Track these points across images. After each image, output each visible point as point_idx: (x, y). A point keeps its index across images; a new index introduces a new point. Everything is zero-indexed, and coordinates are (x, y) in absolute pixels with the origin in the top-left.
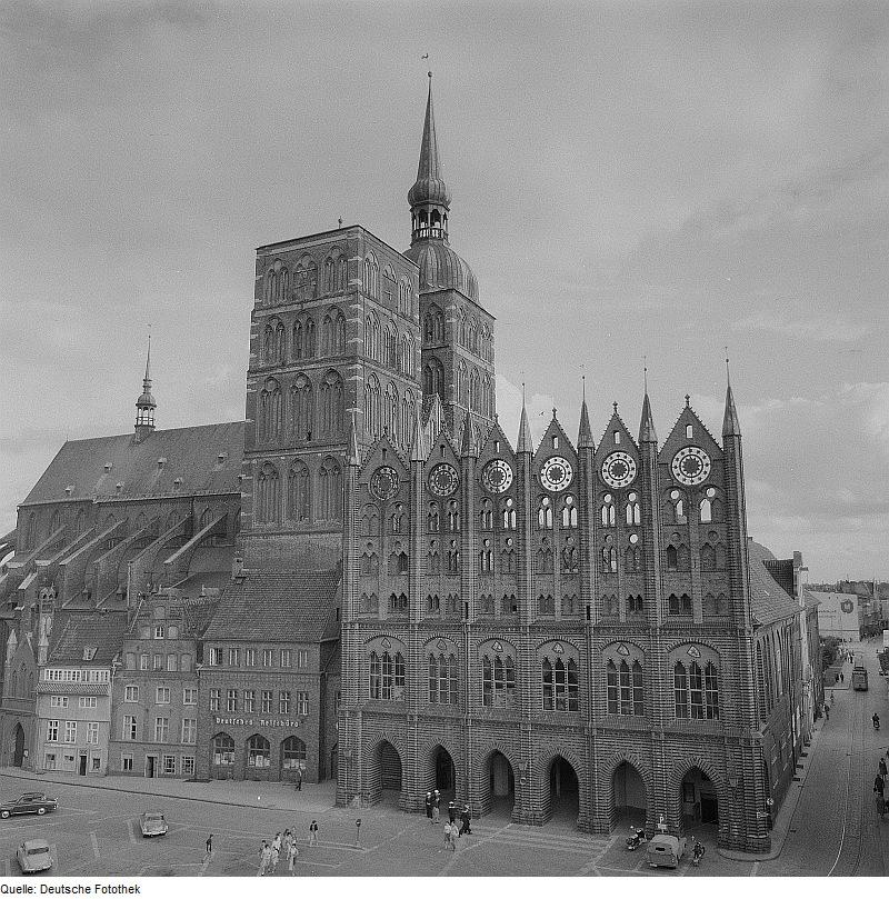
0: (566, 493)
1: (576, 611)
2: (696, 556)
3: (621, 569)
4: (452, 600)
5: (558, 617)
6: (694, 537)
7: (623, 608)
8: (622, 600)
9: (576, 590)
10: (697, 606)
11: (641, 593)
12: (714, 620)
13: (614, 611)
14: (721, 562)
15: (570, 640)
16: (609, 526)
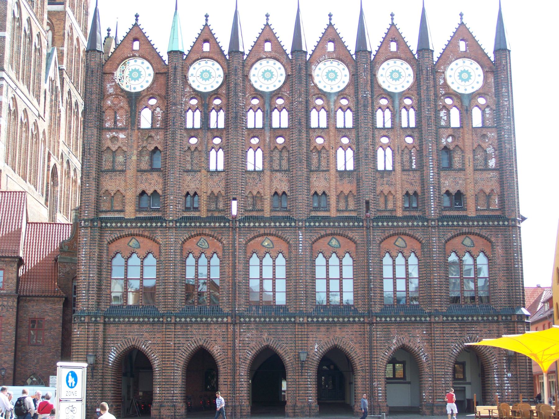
0: (341, 94)
1: (351, 207)
2: (469, 155)
3: (398, 168)
4: (213, 197)
5: (333, 213)
6: (469, 142)
7: (399, 204)
8: (399, 196)
10: (470, 203)
11: (418, 189)
12: (486, 213)
13: (390, 206)
14: (492, 163)
15: (350, 234)
16: (384, 128)
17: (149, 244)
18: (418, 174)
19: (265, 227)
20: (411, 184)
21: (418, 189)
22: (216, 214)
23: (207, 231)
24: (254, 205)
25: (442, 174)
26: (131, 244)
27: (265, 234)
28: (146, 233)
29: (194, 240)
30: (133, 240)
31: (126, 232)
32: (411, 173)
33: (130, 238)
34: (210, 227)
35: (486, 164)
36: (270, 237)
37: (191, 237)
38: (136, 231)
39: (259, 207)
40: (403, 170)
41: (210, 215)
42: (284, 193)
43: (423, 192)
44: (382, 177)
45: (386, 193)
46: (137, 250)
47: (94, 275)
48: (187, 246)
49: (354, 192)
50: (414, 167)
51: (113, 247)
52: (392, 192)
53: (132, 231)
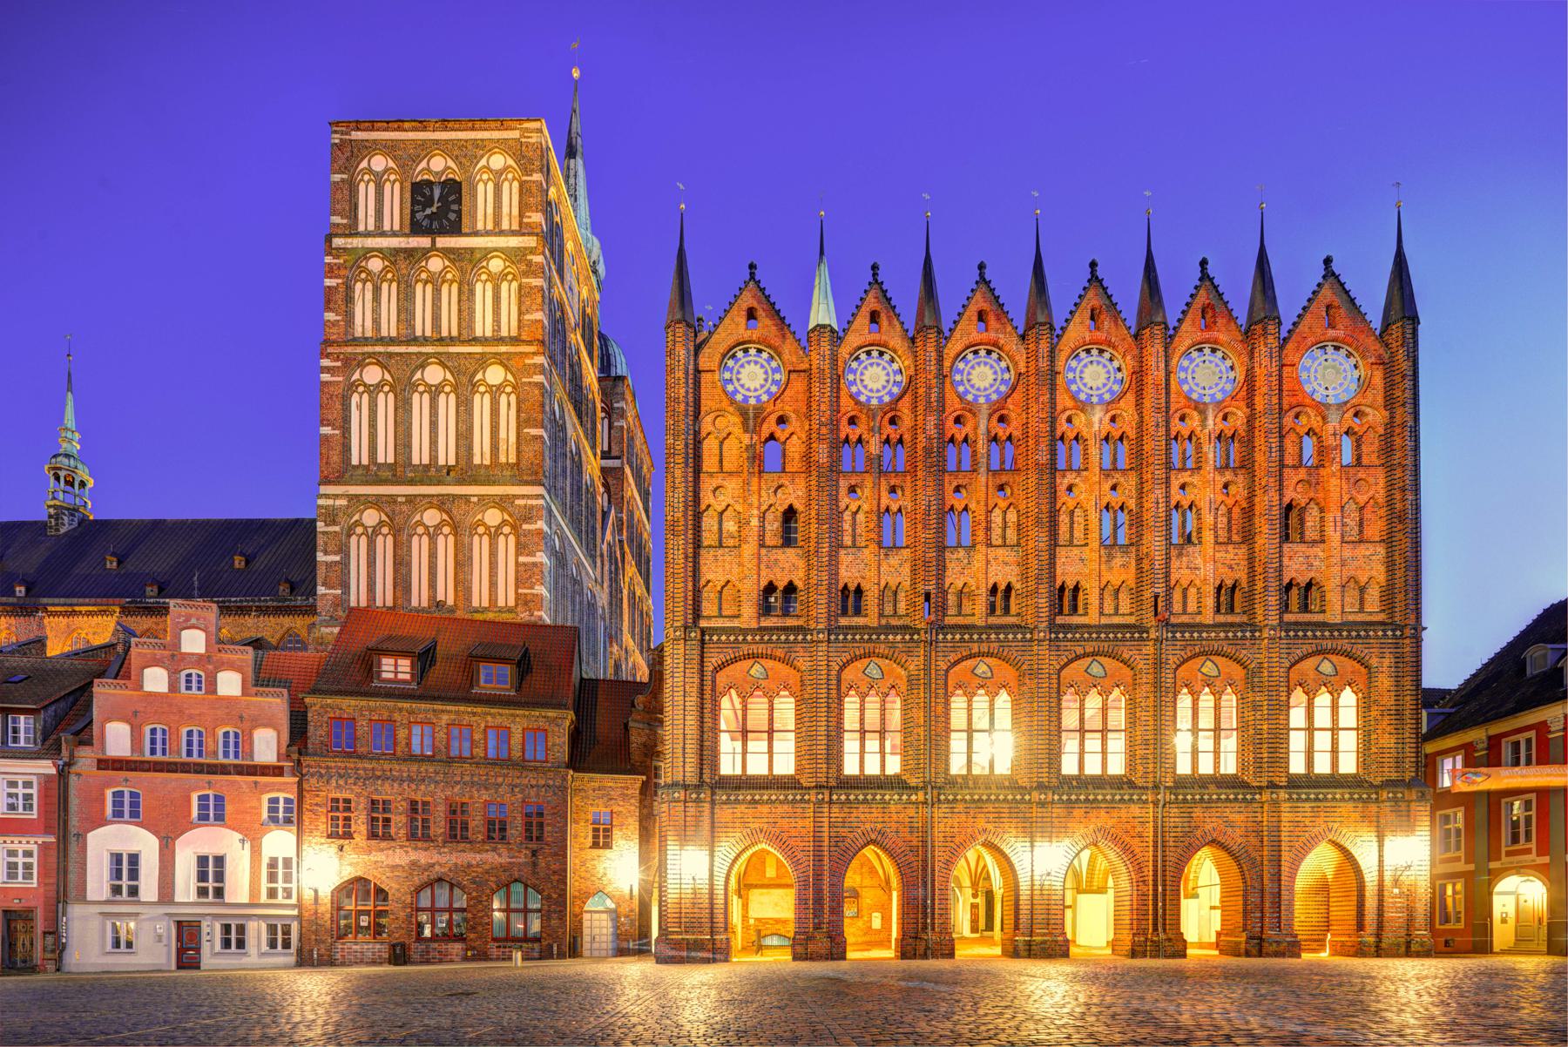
4: (889, 593)
8: (1210, 590)
9: (1130, 577)
17: (783, 669)
18: (1243, 551)
19: (980, 640)
20: (1231, 567)
21: (1242, 575)
22: (894, 622)
23: (882, 649)
24: (960, 606)
25: (1286, 547)
26: (752, 672)
27: (980, 654)
28: (779, 653)
29: (859, 665)
30: (757, 666)
31: (745, 649)
32: (1230, 548)
33: (750, 662)
34: (886, 641)
35: (1361, 532)
36: (986, 660)
37: (856, 658)
38: (761, 648)
39: (967, 609)
40: (1217, 543)
41: (883, 622)
42: (1009, 588)
43: (1252, 582)
44: (1180, 555)
45: (1185, 583)
46: (763, 683)
47: (692, 720)
48: (848, 675)
49: (1132, 583)
50: (1235, 538)
51: (722, 678)
52: (1197, 582)
53: (754, 648)
